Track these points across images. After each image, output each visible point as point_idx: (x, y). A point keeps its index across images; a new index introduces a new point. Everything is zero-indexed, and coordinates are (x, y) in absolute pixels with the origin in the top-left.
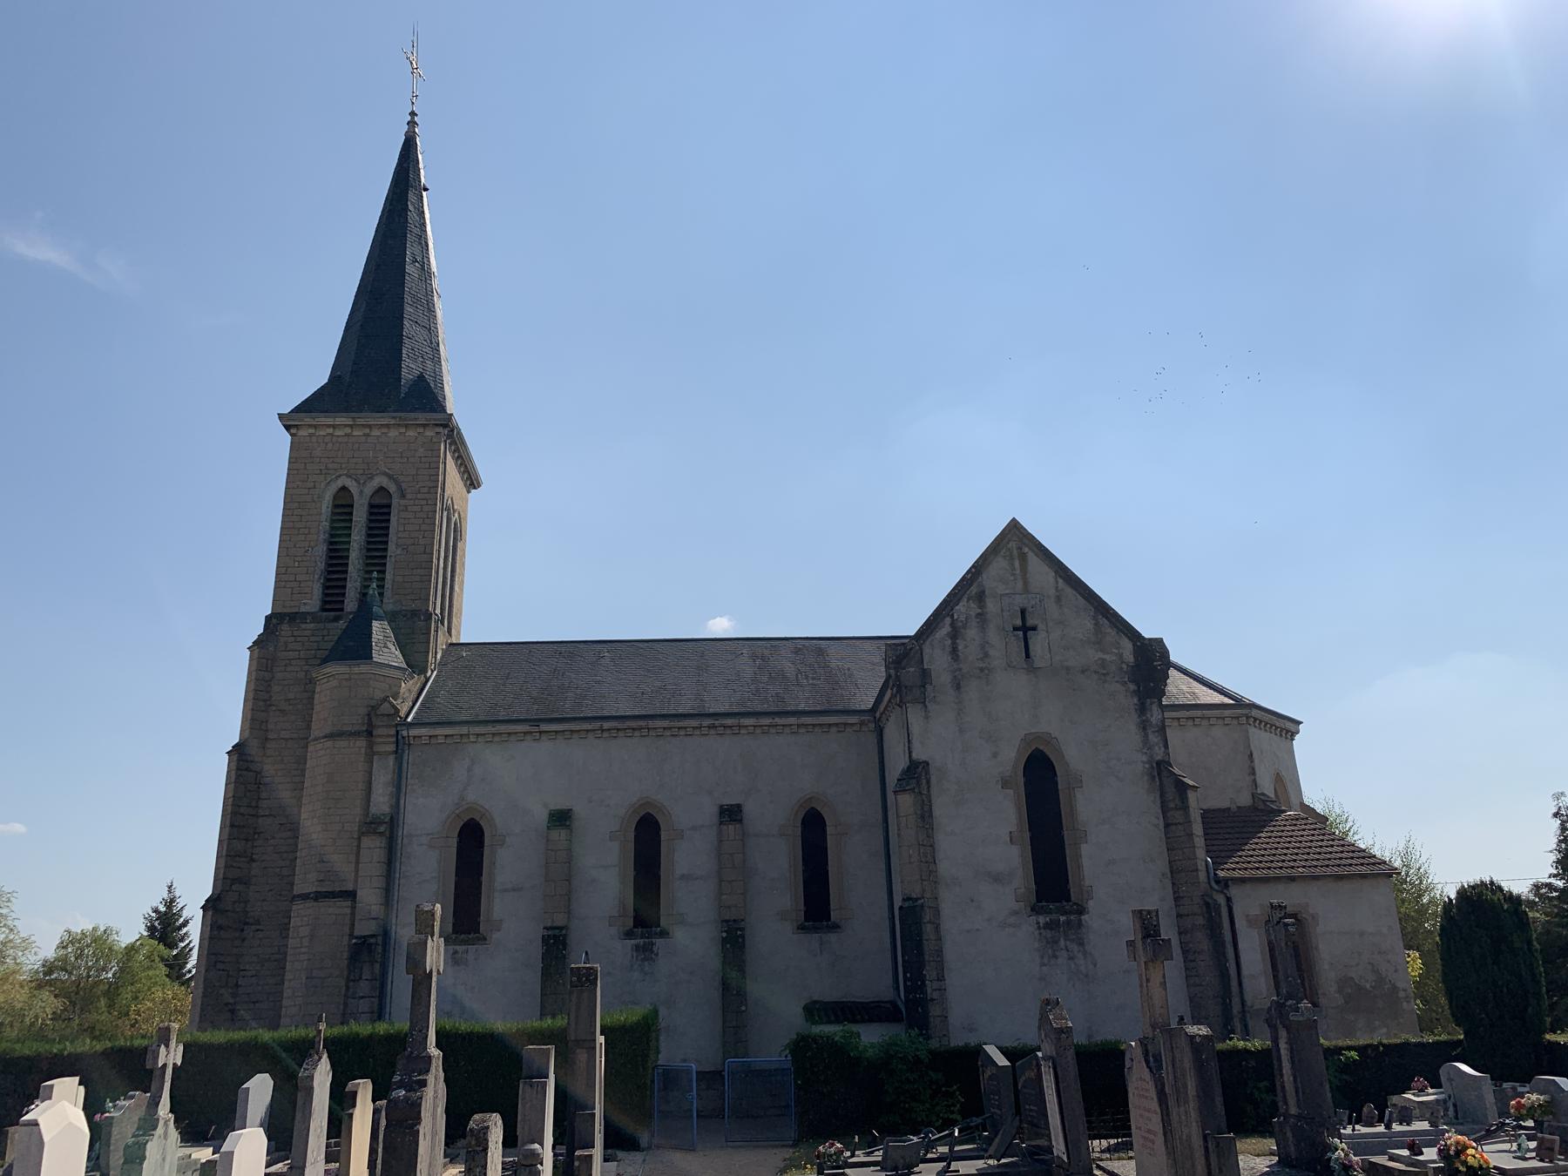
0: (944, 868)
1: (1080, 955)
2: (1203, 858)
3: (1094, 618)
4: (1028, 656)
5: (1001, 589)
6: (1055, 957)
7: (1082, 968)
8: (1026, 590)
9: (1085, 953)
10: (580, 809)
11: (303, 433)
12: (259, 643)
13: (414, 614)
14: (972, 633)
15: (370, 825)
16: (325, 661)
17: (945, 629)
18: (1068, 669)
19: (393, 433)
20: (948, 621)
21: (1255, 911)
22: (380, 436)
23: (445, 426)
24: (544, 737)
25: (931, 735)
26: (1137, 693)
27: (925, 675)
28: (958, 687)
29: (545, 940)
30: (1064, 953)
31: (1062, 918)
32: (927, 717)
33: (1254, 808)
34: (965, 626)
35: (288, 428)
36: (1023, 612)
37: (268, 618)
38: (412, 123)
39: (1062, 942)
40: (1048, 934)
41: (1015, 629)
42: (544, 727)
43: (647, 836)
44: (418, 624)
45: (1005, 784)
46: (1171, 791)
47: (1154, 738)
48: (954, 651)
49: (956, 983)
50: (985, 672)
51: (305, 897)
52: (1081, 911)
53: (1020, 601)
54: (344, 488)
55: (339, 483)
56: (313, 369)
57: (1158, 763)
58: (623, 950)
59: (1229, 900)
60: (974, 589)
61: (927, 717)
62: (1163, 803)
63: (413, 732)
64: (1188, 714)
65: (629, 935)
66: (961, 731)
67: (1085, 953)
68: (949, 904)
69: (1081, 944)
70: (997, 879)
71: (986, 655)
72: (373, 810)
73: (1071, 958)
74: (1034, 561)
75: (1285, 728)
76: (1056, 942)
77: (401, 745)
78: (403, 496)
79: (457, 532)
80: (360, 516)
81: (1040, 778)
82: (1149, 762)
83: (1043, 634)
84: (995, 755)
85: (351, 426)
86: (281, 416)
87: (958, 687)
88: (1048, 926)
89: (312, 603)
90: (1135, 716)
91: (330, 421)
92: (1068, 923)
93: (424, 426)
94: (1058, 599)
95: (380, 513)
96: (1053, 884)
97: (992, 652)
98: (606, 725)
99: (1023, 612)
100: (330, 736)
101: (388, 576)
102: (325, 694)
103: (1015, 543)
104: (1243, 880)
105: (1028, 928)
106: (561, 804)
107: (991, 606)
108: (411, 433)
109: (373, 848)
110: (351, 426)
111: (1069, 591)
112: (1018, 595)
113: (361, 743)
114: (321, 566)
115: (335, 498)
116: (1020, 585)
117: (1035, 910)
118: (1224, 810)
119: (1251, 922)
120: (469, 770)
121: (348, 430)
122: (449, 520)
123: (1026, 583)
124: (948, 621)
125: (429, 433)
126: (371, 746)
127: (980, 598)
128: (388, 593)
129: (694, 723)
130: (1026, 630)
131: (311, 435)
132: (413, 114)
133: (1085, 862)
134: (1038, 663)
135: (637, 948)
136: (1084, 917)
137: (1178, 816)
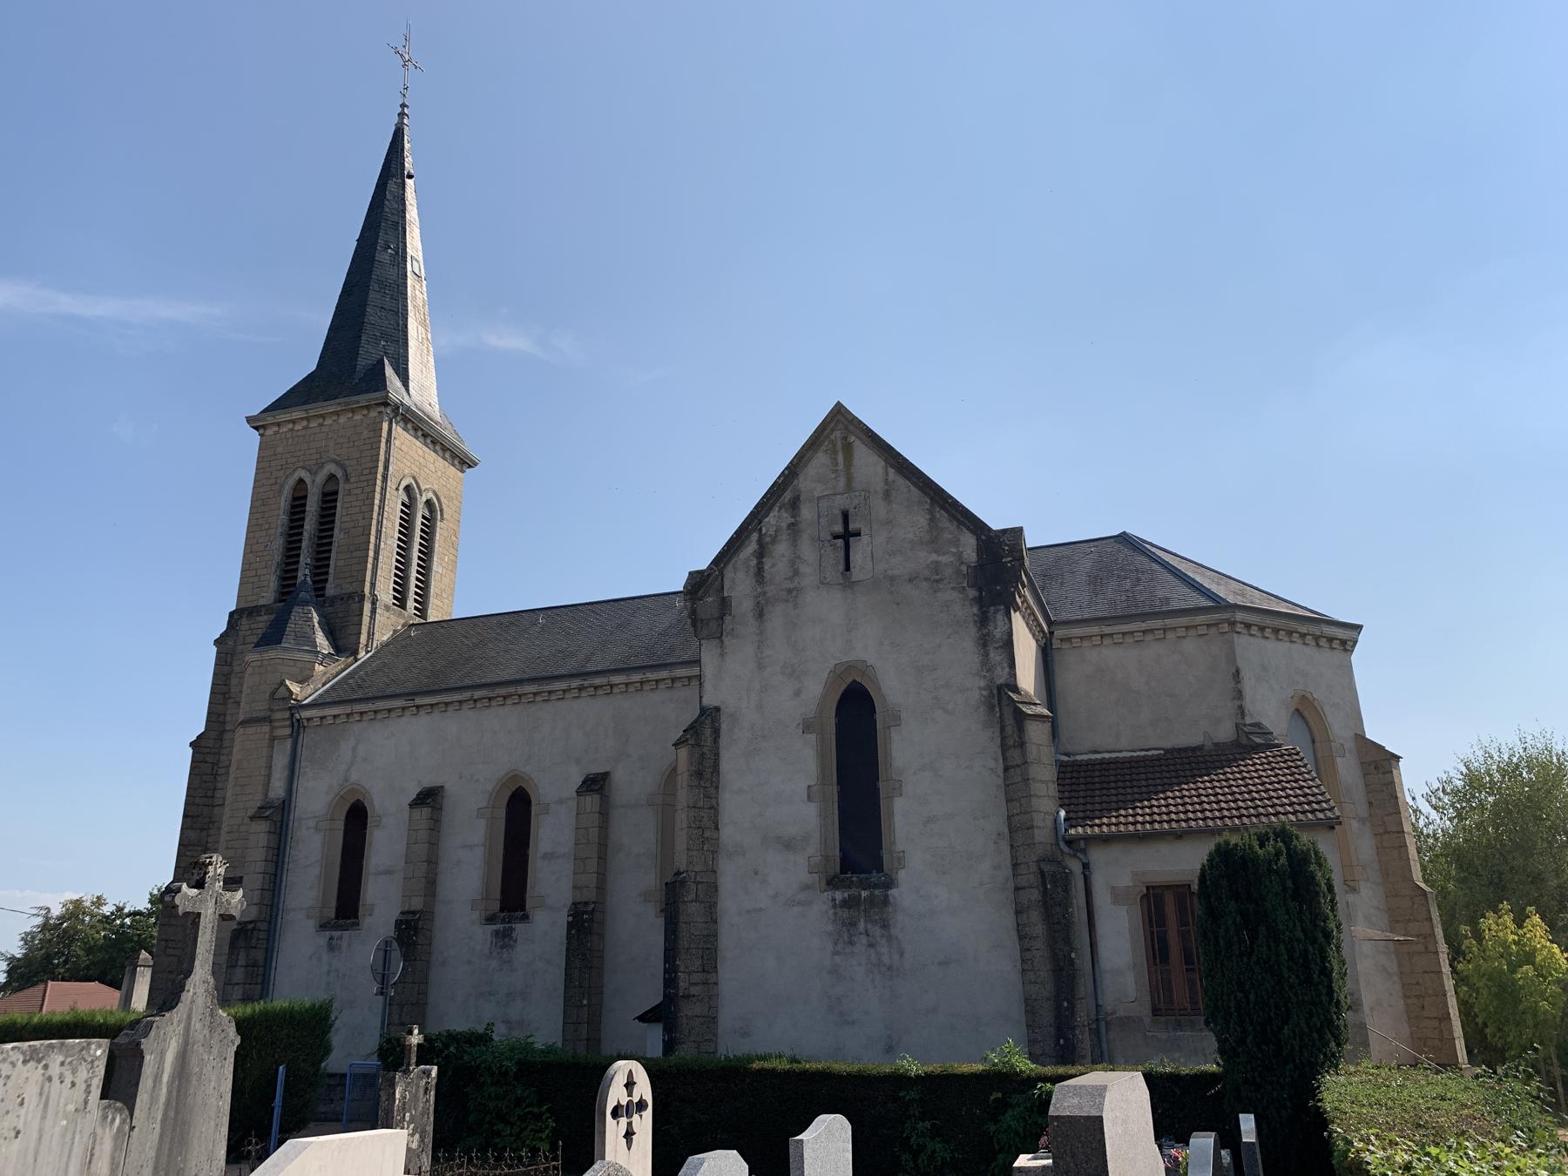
0: (729, 833)
1: (883, 941)
2: (1047, 808)
3: (931, 512)
4: (848, 568)
5: (819, 490)
6: (851, 943)
7: (886, 959)
9: (890, 938)
10: (452, 787)
11: (269, 432)
13: (350, 596)
14: (782, 548)
17: (751, 547)
18: (892, 579)
19: (342, 420)
20: (755, 536)
21: (1125, 881)
22: (335, 422)
23: (386, 404)
24: (422, 712)
25: (728, 676)
26: (979, 601)
27: (724, 605)
28: (760, 615)
29: (398, 924)
30: (864, 940)
31: (864, 894)
32: (722, 655)
33: (1236, 744)
34: (774, 540)
35: (256, 428)
36: (846, 516)
37: (231, 614)
39: (862, 925)
40: (845, 913)
41: (836, 537)
42: (419, 701)
43: (518, 809)
45: (807, 727)
46: (1010, 721)
47: (996, 656)
48: (760, 571)
49: (729, 975)
50: (793, 594)
52: (889, 884)
53: (841, 502)
54: (301, 481)
55: (296, 476)
57: (1000, 688)
58: (483, 935)
59: (1086, 866)
60: (788, 496)
61: (722, 655)
62: (1003, 739)
63: (306, 714)
64: (1144, 626)
65: (490, 920)
66: (761, 667)
67: (890, 938)
68: (729, 876)
69: (885, 926)
70: (788, 845)
71: (796, 573)
72: (272, 795)
73: (871, 945)
74: (862, 453)
75: (1338, 637)
76: (853, 924)
77: (297, 727)
78: (347, 480)
80: (312, 506)
81: (855, 719)
82: (989, 688)
83: (865, 539)
84: (798, 693)
85: (307, 419)
86: (249, 420)
87: (760, 615)
88: (845, 904)
89: (268, 596)
90: (973, 630)
91: (287, 417)
92: (871, 901)
93: (367, 407)
94: (887, 495)
95: (329, 500)
96: (859, 851)
97: (803, 569)
98: (478, 694)
99: (846, 516)
103: (841, 431)
104: (1106, 840)
105: (820, 908)
106: (429, 781)
107: (807, 513)
108: (358, 417)
110: (307, 419)
111: (902, 483)
112: (846, 495)
114: (277, 558)
115: (295, 489)
116: (842, 484)
117: (832, 883)
118: (1194, 749)
119: (1118, 896)
120: (354, 749)
121: (305, 423)
123: (849, 480)
124: (755, 536)
125: (373, 414)
127: (794, 505)
129: (562, 685)
130: (847, 536)
131: (276, 433)
132: (403, 106)
133: (898, 820)
134: (856, 574)
135: (497, 933)
136: (893, 892)
137: (1015, 755)
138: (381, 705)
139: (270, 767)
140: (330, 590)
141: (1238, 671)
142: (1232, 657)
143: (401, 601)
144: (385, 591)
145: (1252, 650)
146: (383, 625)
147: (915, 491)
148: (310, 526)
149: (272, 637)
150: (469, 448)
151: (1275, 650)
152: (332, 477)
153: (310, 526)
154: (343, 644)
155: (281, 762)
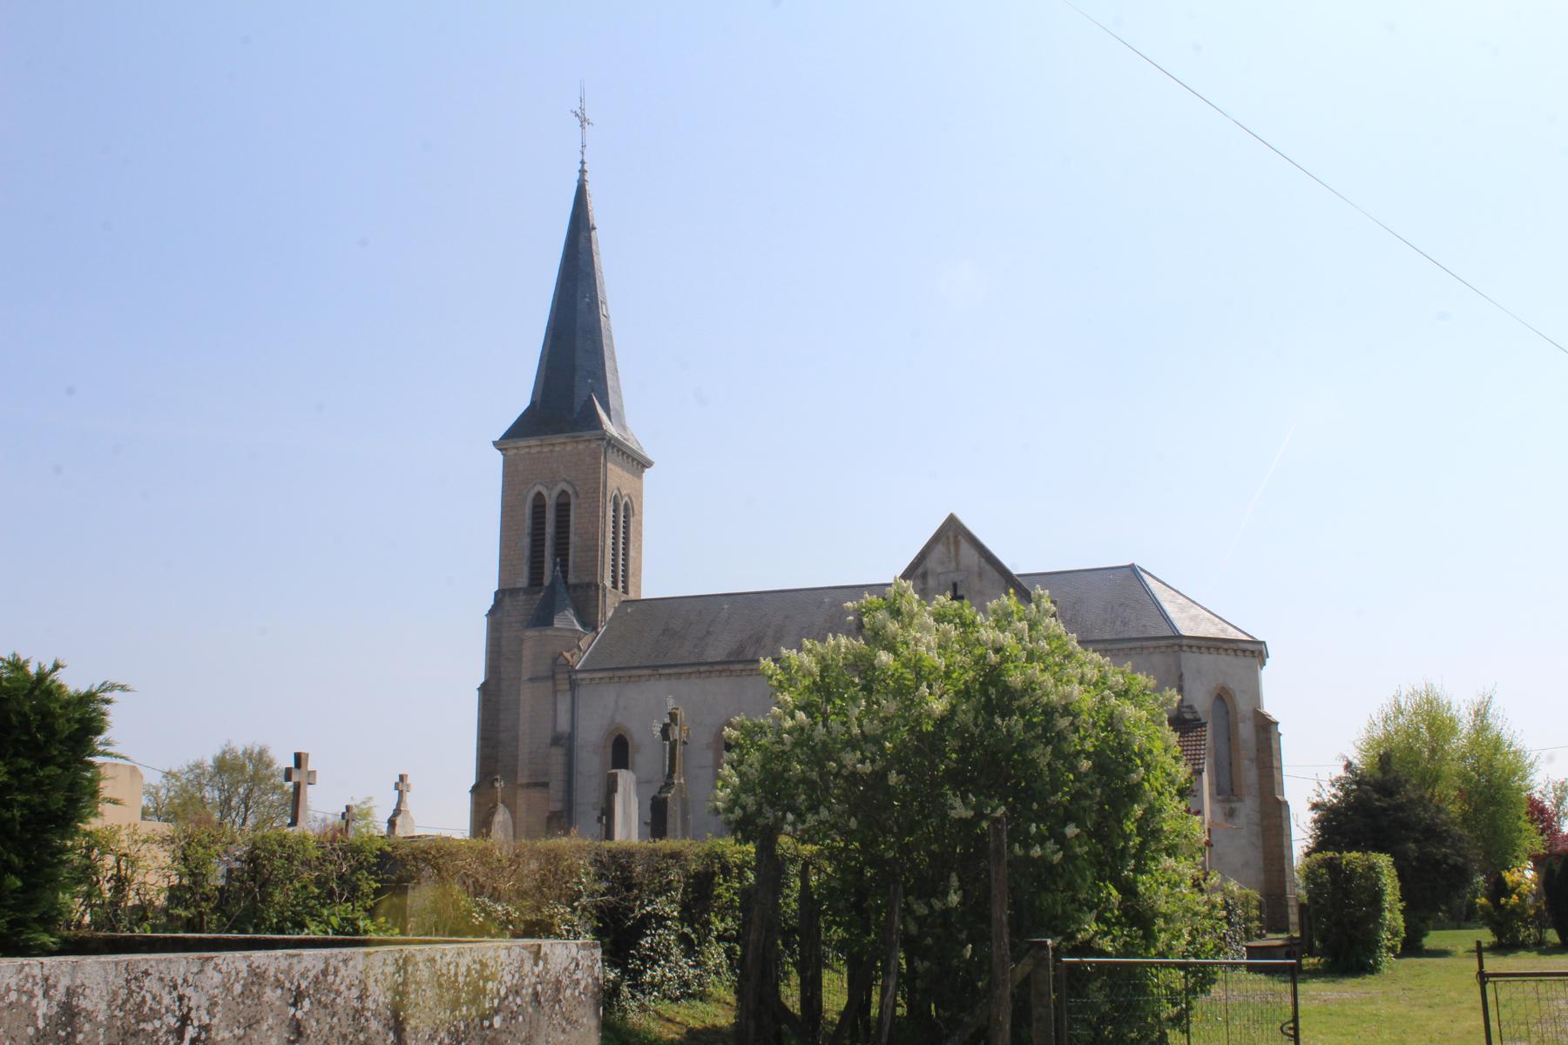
5: (939, 569)
8: (957, 569)
11: (511, 452)
12: (492, 613)
13: (589, 585)
15: (556, 740)
16: (527, 627)
19: (569, 448)
22: (561, 448)
37: (496, 594)
38: (583, 172)
42: (661, 671)
44: (585, 600)
51: (522, 786)
54: (539, 494)
56: (515, 392)
60: (920, 570)
63: (580, 676)
74: (965, 547)
77: (573, 685)
78: (577, 496)
79: (626, 514)
80: (550, 516)
86: (495, 443)
89: (523, 581)
94: (980, 575)
95: (563, 509)
98: (702, 669)
100: (531, 680)
101: (571, 559)
102: (527, 652)
103: (953, 533)
108: (581, 447)
109: (557, 755)
111: (988, 568)
113: (550, 683)
114: (527, 553)
116: (953, 565)
122: (616, 505)
123: (958, 564)
125: (593, 445)
126: (555, 685)
127: (924, 576)
128: (571, 570)
132: (583, 163)
138: (634, 672)
139: (555, 710)
140: (572, 579)
141: (1181, 676)
142: (1179, 667)
143: (615, 586)
144: (608, 583)
145: (1190, 661)
146: (610, 603)
147: (996, 575)
148: (550, 529)
149: (543, 618)
150: (649, 453)
151: (1207, 659)
152: (564, 492)
153: (550, 529)
154: (589, 623)
155: (563, 704)
